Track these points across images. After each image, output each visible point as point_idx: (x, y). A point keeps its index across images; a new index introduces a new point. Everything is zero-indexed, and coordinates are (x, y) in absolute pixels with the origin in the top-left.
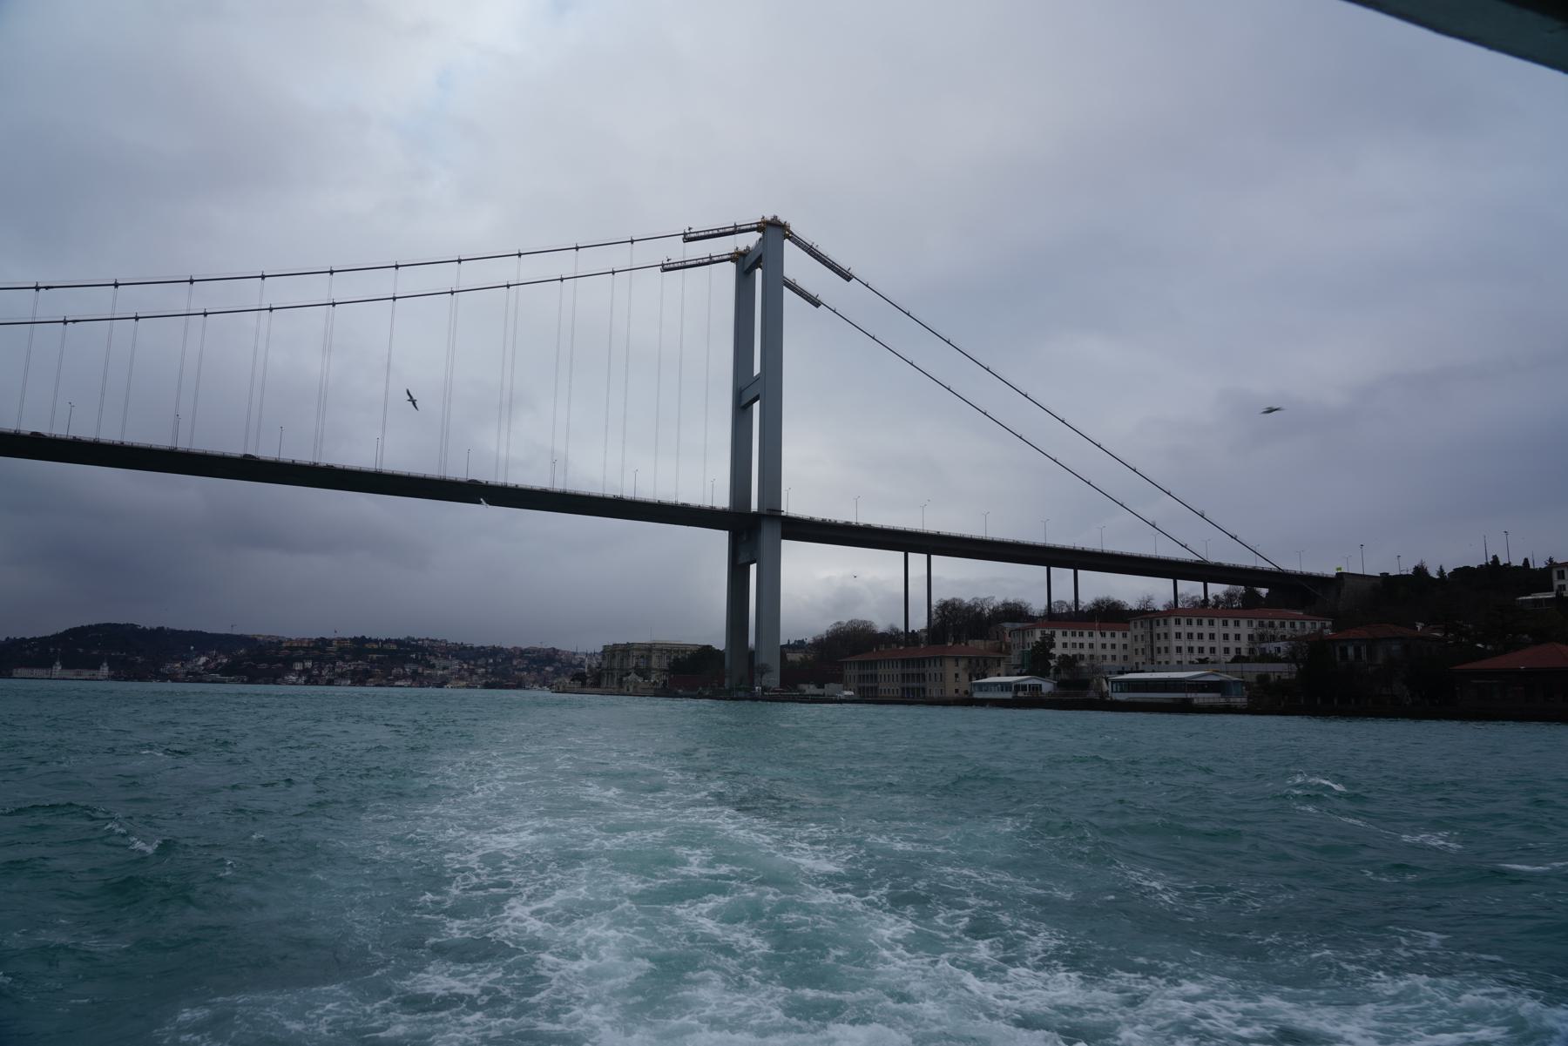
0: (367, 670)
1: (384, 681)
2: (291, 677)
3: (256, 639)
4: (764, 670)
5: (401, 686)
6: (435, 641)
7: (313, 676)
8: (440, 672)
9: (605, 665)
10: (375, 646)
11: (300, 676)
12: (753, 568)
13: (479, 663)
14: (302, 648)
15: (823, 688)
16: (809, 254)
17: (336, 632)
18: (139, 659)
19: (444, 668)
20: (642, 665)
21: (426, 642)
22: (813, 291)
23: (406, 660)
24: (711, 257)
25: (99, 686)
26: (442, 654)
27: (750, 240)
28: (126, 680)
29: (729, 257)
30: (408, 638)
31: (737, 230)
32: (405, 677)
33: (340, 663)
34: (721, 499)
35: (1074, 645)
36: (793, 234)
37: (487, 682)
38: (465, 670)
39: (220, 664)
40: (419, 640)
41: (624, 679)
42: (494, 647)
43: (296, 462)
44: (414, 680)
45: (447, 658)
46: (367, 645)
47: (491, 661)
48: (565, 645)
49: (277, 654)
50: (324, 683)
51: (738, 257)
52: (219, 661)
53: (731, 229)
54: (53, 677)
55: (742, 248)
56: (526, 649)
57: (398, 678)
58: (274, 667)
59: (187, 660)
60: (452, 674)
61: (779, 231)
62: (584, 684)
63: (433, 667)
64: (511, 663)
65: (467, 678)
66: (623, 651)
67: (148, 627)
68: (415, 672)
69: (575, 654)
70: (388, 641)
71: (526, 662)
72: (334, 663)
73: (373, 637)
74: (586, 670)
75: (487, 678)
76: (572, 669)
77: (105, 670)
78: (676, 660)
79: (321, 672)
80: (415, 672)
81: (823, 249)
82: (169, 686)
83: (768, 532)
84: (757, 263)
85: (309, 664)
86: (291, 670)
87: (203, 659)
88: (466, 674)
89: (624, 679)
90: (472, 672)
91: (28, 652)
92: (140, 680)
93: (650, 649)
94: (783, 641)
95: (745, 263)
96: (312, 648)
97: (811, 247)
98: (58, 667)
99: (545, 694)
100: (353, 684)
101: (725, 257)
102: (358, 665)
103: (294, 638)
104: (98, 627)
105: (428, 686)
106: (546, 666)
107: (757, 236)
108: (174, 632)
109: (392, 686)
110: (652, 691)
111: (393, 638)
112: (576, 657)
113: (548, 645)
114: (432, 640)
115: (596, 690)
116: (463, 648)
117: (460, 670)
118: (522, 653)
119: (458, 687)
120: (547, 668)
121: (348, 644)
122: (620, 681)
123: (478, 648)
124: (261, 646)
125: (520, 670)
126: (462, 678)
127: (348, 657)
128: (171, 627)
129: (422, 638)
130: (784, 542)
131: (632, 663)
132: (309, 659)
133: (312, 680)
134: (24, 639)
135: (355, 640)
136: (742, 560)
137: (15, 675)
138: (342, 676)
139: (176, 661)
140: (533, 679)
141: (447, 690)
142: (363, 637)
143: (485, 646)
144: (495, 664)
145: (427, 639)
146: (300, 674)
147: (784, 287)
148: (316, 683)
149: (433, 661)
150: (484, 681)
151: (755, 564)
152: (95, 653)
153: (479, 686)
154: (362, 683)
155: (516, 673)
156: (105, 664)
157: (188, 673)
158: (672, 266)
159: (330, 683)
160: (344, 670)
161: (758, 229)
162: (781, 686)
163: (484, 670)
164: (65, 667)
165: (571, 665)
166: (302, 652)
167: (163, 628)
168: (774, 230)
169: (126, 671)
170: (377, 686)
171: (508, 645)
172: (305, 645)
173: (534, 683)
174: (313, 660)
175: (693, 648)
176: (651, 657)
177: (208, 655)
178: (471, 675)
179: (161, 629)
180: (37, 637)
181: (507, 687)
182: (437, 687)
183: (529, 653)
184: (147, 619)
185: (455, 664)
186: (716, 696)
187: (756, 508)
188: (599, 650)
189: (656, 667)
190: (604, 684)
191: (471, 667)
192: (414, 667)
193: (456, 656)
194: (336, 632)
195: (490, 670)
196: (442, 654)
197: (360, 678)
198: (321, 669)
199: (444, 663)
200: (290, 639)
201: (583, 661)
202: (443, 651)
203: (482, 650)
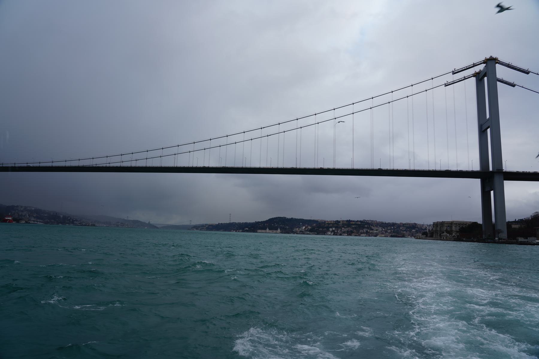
0: (352, 230)
1: (357, 234)
2: (329, 233)
3: (318, 221)
4: (500, 231)
5: (363, 236)
6: (373, 221)
8: (375, 232)
9: (434, 229)
10: (354, 223)
12: (492, 192)
13: (388, 228)
15: (527, 239)
16: (508, 67)
18: (287, 227)
20: (449, 229)
21: (370, 221)
22: (511, 81)
23: (364, 228)
24: (464, 77)
25: (277, 236)
27: (482, 67)
29: (472, 75)
30: (364, 220)
31: (474, 65)
32: (364, 233)
33: (343, 228)
34: (476, 167)
36: (499, 61)
37: (391, 235)
38: (384, 231)
40: (368, 221)
41: (442, 234)
43: (398, 169)
44: (367, 234)
45: (377, 227)
46: (351, 223)
48: (419, 222)
49: (325, 225)
50: (339, 235)
51: (476, 75)
52: (308, 228)
53: (472, 66)
55: (478, 71)
57: (362, 233)
59: (300, 228)
60: (379, 232)
61: (493, 62)
62: (427, 236)
63: (373, 230)
64: (400, 228)
65: (385, 233)
66: (441, 224)
67: (289, 218)
68: (367, 232)
69: (423, 225)
70: (358, 221)
72: (341, 229)
73: (353, 220)
74: (428, 231)
75: (391, 234)
76: (423, 231)
77: (279, 230)
78: (462, 227)
79: (338, 231)
80: (367, 232)
81: (514, 64)
82: (295, 235)
83: (497, 179)
84: (485, 75)
85: (334, 229)
86: (328, 230)
87: (304, 227)
88: (384, 232)
89: (442, 234)
90: (386, 232)
91: (260, 225)
93: (451, 224)
94: (507, 221)
95: (479, 77)
97: (509, 64)
98: (268, 230)
99: (413, 239)
100: (348, 235)
101: (471, 76)
105: (372, 236)
106: (412, 230)
107: (483, 65)
108: (295, 219)
110: (453, 239)
111: (359, 220)
112: (424, 226)
113: (412, 221)
114: (372, 221)
115: (431, 238)
116: (382, 223)
118: (404, 225)
119: (382, 237)
120: (413, 230)
122: (440, 235)
124: (320, 223)
125: (403, 231)
126: (383, 234)
127: (345, 226)
128: (295, 218)
130: (505, 182)
131: (445, 228)
132: (334, 227)
133: (335, 234)
134: (259, 222)
135: (347, 221)
138: (344, 232)
139: (297, 228)
140: (408, 234)
141: (378, 237)
142: (350, 220)
144: (394, 229)
145: (370, 220)
147: (497, 82)
148: (336, 235)
149: (373, 228)
151: (493, 191)
155: (402, 232)
156: (279, 229)
157: (300, 232)
158: (449, 84)
159: (340, 235)
160: (345, 231)
161: (484, 63)
162: (508, 237)
163: (390, 231)
164: (270, 229)
165: (422, 229)
168: (491, 62)
169: (285, 231)
170: (355, 236)
171: (398, 222)
172: (332, 223)
173: (408, 235)
174: (335, 227)
175: (469, 223)
176: (452, 226)
179: (292, 218)
181: (399, 237)
182: (375, 236)
183: (406, 225)
184: (289, 215)
185: (380, 229)
186: (478, 241)
187: (492, 169)
189: (454, 230)
190: (434, 236)
191: (386, 230)
193: (380, 226)
195: (392, 231)
197: (350, 233)
198: (338, 230)
199: (376, 228)
200: (328, 221)
201: (426, 228)
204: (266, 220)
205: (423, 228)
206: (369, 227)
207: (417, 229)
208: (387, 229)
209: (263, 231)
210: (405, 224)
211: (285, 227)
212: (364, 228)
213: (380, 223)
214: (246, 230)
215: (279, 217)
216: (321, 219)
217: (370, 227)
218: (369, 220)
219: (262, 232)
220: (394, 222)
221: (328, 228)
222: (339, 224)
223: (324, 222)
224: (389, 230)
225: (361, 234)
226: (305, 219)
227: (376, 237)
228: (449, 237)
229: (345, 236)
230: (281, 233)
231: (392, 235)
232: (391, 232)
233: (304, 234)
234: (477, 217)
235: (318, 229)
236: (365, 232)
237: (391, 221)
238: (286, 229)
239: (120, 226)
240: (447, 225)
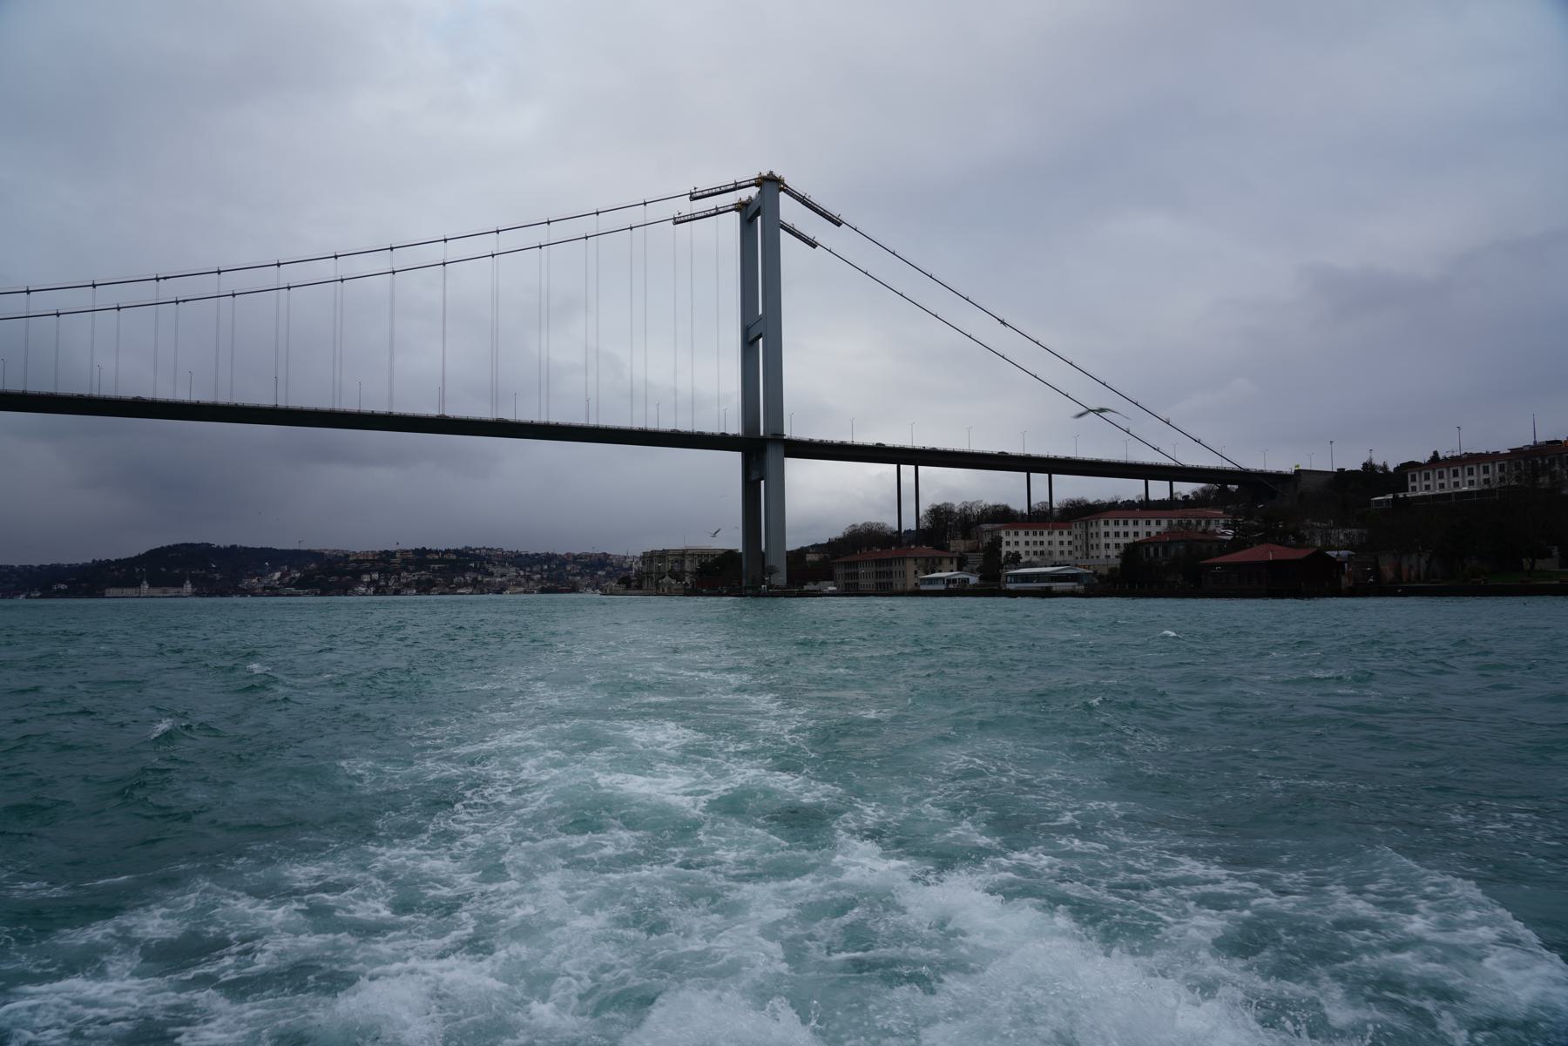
1: (447, 590)
2: (360, 588)
6: (491, 550)
7: (380, 587)
8: (498, 580)
10: (436, 557)
11: (368, 587)
12: (762, 482)
13: (535, 569)
14: (368, 560)
19: (503, 575)
20: (677, 569)
23: (465, 569)
24: (717, 209)
26: (499, 561)
27: (753, 192)
29: (733, 207)
30: (466, 548)
31: (737, 187)
32: (466, 585)
34: (734, 427)
35: (1035, 543)
36: (787, 186)
37: (543, 588)
39: (294, 578)
40: (477, 549)
41: (660, 581)
44: (475, 587)
45: (504, 566)
48: (616, 550)
49: (346, 567)
51: (741, 207)
52: (292, 576)
53: (732, 187)
54: (142, 595)
55: (744, 199)
56: (578, 555)
57: (459, 586)
58: (344, 579)
59: (262, 576)
61: (775, 185)
62: (628, 587)
63: (491, 574)
64: (565, 568)
68: (475, 579)
69: (625, 557)
70: (448, 551)
71: (579, 567)
75: (542, 583)
76: (623, 573)
77: (188, 587)
80: (475, 579)
81: (815, 199)
82: (249, 599)
83: (772, 453)
85: (376, 576)
86: (359, 582)
87: (278, 575)
88: (523, 580)
89: (660, 581)
90: (528, 579)
91: (116, 573)
92: (222, 595)
95: (748, 212)
96: (377, 560)
97: (804, 197)
98: (145, 587)
99: (597, 596)
100: (419, 593)
101: (730, 208)
102: (422, 575)
104: (176, 548)
105: (488, 593)
110: (682, 591)
111: (452, 547)
112: (627, 560)
113: (599, 550)
114: (488, 549)
115: (637, 591)
117: (516, 576)
118: (576, 559)
119: (516, 593)
120: (600, 573)
122: (657, 585)
123: (532, 555)
124: (328, 560)
125: (575, 575)
126: (519, 584)
127: (411, 568)
131: (668, 566)
132: (375, 571)
134: (108, 561)
135: (416, 551)
136: (754, 477)
137: (107, 595)
138: (408, 585)
139: (252, 577)
141: (506, 596)
142: (424, 548)
145: (484, 548)
146: (368, 585)
148: (384, 593)
149: (491, 569)
154: (426, 591)
155: (570, 578)
156: (188, 582)
157: (265, 588)
158: (682, 219)
159: (397, 592)
160: (409, 580)
161: (756, 185)
164: (152, 585)
166: (368, 565)
168: (770, 184)
169: (208, 588)
170: (440, 594)
171: (561, 551)
172: (370, 558)
173: (587, 586)
174: (380, 571)
175: (721, 552)
181: (562, 592)
183: (581, 558)
184: (221, 539)
185: (512, 572)
188: (639, 554)
189: (689, 570)
190: (645, 587)
192: (473, 575)
193: (512, 564)
195: (545, 576)
196: (499, 561)
197: (424, 588)
198: (387, 580)
199: (501, 570)
205: (624, 565)
206: (480, 568)
207: (608, 568)
210: (580, 557)
215: (186, 545)
216: (331, 547)
217: (484, 568)
218: (481, 547)
219: (124, 594)
221: (356, 576)
224: (537, 573)
226: (279, 547)
228: (676, 587)
229: (410, 594)
230: (197, 594)
231: (546, 587)
233: (277, 595)
234: (732, 539)
235: (324, 577)
236: (469, 581)
237: (542, 549)
240: (673, 558)
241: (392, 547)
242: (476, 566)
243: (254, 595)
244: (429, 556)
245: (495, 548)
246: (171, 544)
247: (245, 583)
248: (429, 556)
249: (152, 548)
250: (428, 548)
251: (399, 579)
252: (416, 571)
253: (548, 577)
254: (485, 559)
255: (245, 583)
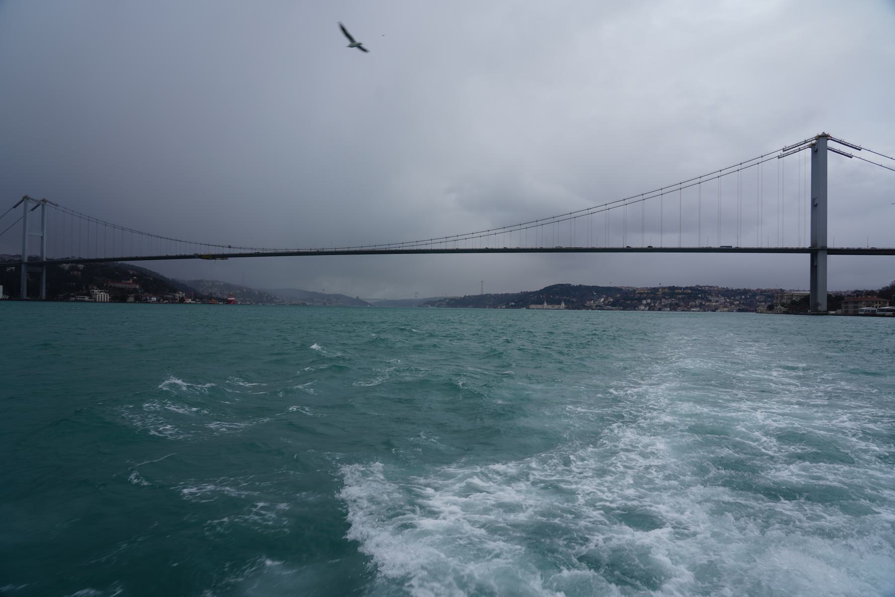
1: (686, 309)
3: (622, 289)
6: (711, 287)
8: (714, 304)
10: (680, 291)
11: (646, 306)
13: (737, 298)
14: (645, 293)
17: (660, 284)
18: (575, 300)
19: (716, 302)
23: (696, 298)
26: (716, 294)
28: (573, 309)
30: (697, 286)
32: (696, 306)
38: (728, 302)
39: (610, 301)
40: (703, 286)
42: (745, 289)
44: (701, 308)
45: (718, 296)
47: (744, 297)
56: (764, 290)
57: (692, 307)
58: (633, 302)
60: (721, 304)
63: (710, 301)
67: (575, 285)
68: (701, 304)
70: (686, 288)
71: (764, 297)
75: (740, 306)
77: (563, 305)
80: (701, 304)
85: (649, 301)
88: (729, 304)
90: (731, 304)
92: (578, 309)
100: (671, 310)
103: (639, 288)
105: (708, 311)
108: (586, 286)
109: (690, 311)
114: (709, 287)
117: (725, 302)
118: (762, 292)
121: (667, 290)
123: (736, 290)
126: (725, 307)
127: (667, 297)
128: (585, 285)
129: (704, 285)
133: (651, 308)
135: (670, 288)
137: (530, 308)
138: (665, 306)
139: (591, 300)
143: (740, 288)
145: (707, 286)
146: (646, 305)
148: (653, 310)
149: (710, 298)
150: (738, 308)
152: (557, 297)
153: (735, 311)
157: (597, 306)
159: (660, 310)
163: (738, 302)
164: (548, 304)
166: (645, 295)
167: (581, 285)
170: (682, 311)
171: (754, 287)
172: (646, 291)
174: (651, 299)
177: (603, 297)
178: (731, 305)
179: (580, 285)
180: (532, 291)
181: (750, 311)
182: (713, 311)
183: (766, 292)
184: (575, 282)
185: (722, 300)
191: (731, 301)
192: (701, 301)
193: (723, 295)
194: (660, 284)
195: (742, 302)
196: (716, 294)
197: (674, 307)
198: (655, 303)
199: (716, 299)
202: (716, 292)
203: (738, 291)
204: (540, 289)
208: (733, 300)
209: (539, 306)
210: (765, 291)
211: (571, 300)
212: (696, 299)
213: (724, 290)
214: (512, 306)
216: (626, 286)
218: (706, 285)
220: (746, 288)
221: (640, 300)
222: (658, 293)
223: (634, 291)
225: (692, 308)
227: (715, 311)
230: (567, 308)
232: (740, 303)
233: (602, 309)
237: (742, 287)
238: (573, 302)
239: (328, 305)
241: (657, 286)
242: (701, 296)
243: (592, 309)
244: (676, 291)
245: (714, 286)
246: (554, 284)
247: (588, 303)
248: (676, 291)
249: (547, 286)
250: (676, 286)
251: (661, 303)
252: (670, 298)
253: (743, 303)
254: (707, 292)
255: (588, 303)
